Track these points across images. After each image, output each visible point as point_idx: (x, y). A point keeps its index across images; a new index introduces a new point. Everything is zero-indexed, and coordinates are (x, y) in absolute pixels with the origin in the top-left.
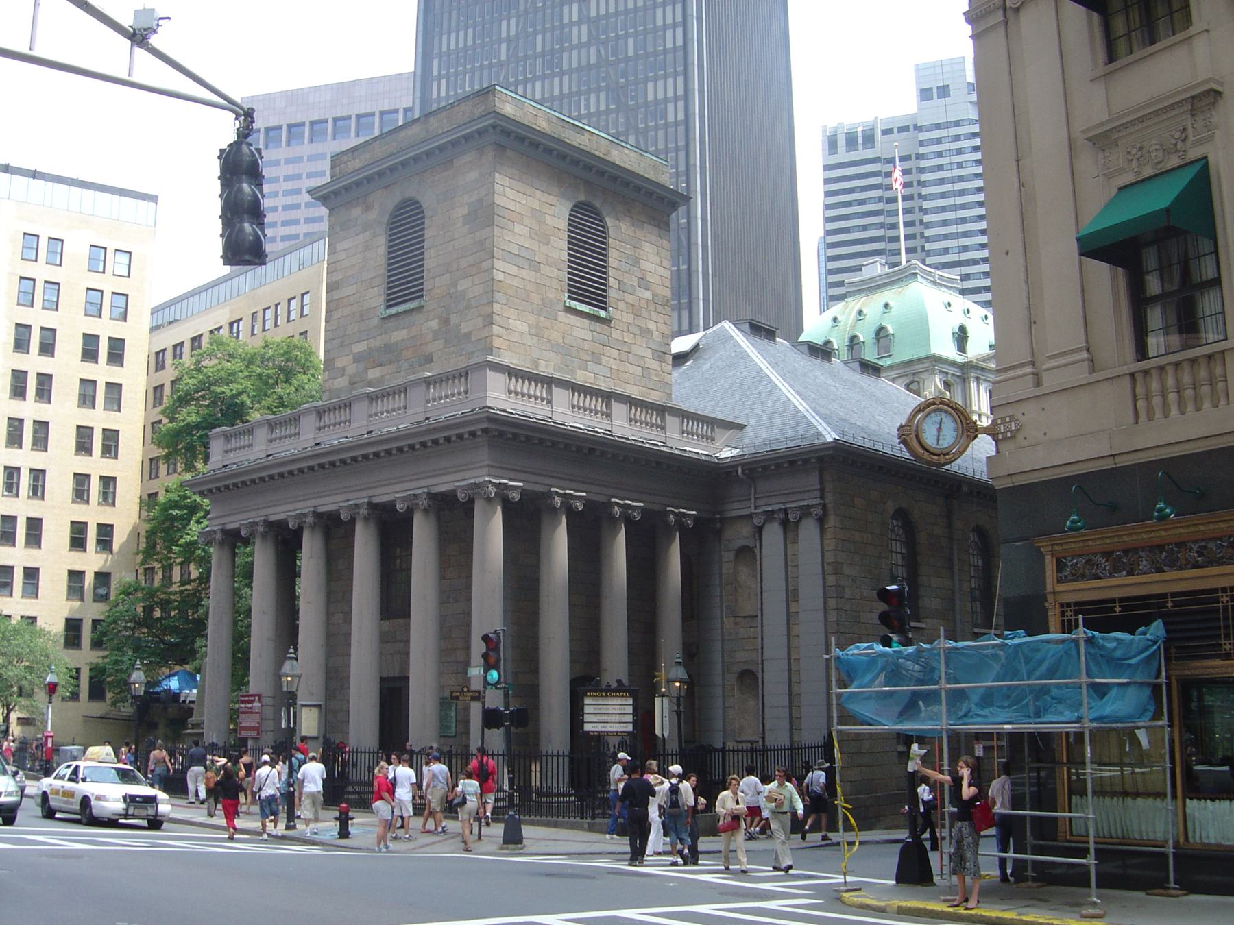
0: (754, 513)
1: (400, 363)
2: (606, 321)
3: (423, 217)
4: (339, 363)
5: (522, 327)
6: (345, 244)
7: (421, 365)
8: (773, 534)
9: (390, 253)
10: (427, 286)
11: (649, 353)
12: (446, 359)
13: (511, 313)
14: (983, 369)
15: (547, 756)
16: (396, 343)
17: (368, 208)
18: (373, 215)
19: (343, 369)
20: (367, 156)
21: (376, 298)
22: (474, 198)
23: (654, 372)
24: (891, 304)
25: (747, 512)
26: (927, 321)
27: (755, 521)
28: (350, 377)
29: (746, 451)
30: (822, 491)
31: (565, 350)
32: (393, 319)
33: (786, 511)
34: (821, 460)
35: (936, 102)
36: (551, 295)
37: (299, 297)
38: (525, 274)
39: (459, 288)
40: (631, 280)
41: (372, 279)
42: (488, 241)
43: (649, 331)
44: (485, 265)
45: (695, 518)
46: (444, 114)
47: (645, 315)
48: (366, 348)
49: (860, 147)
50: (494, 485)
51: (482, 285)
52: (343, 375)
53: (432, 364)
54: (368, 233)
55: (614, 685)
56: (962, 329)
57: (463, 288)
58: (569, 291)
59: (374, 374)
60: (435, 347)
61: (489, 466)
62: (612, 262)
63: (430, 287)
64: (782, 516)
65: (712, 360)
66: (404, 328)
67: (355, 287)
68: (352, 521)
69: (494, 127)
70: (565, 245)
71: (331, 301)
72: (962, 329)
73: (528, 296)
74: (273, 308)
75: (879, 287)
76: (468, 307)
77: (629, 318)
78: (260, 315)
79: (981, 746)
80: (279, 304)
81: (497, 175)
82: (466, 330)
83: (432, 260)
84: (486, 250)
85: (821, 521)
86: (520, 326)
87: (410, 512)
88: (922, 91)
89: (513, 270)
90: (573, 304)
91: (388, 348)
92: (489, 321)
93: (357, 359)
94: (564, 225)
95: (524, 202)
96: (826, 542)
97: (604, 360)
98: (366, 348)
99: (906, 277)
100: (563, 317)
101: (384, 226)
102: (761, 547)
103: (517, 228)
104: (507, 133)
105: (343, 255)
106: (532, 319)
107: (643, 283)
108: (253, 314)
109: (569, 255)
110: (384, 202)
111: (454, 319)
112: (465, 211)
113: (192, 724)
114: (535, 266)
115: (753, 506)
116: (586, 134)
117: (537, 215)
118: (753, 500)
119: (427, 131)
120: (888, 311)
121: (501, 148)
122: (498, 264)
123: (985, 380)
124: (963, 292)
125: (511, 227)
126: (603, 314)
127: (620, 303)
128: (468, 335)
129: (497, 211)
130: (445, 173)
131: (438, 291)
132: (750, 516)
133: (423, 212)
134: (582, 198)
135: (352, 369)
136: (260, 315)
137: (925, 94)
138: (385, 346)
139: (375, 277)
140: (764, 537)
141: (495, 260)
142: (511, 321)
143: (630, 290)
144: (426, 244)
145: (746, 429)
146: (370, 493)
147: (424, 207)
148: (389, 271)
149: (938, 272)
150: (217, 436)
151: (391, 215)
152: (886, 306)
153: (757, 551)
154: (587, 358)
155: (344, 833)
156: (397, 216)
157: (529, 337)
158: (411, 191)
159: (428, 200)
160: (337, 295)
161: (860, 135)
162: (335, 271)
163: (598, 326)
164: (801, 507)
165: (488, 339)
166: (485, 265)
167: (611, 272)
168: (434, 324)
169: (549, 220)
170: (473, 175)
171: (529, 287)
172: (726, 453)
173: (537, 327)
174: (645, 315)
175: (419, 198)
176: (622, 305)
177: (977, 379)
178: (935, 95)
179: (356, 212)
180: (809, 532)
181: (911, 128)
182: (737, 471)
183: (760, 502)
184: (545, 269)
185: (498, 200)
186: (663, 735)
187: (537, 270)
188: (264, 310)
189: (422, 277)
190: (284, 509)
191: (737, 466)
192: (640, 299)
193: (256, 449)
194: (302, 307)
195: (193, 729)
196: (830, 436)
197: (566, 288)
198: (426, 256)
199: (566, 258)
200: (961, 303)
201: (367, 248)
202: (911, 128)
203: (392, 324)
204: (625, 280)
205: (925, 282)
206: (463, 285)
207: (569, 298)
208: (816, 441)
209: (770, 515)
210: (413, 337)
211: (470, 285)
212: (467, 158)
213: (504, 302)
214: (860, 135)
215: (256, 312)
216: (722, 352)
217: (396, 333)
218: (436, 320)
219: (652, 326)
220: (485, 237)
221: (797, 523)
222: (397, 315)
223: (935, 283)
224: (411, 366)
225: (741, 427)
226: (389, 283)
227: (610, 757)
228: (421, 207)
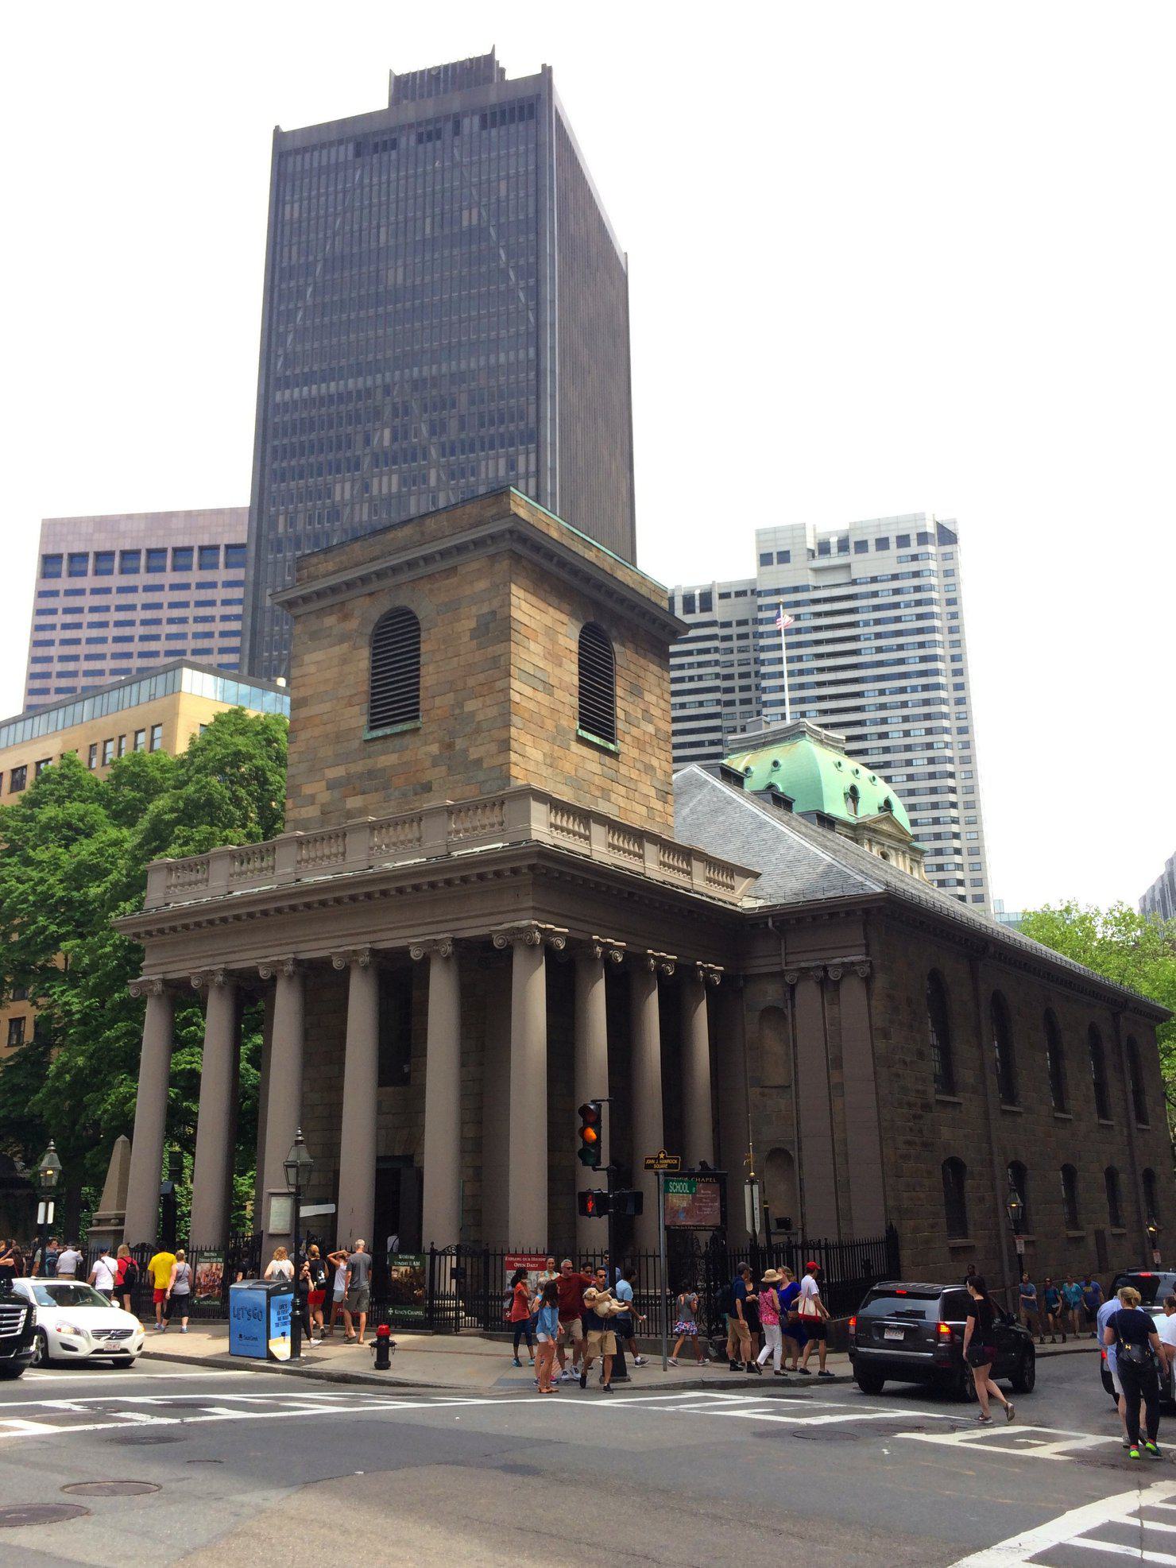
0: (787, 970)
2: (614, 755)
3: (419, 629)
4: (307, 790)
5: (535, 754)
6: (319, 656)
7: (416, 794)
8: (808, 995)
9: (374, 668)
10: (423, 706)
11: (652, 792)
12: (449, 788)
13: (526, 739)
14: (875, 831)
15: (647, 1256)
16: (384, 769)
17: (346, 617)
18: (353, 624)
19: (313, 797)
20: (344, 558)
21: (357, 717)
22: (485, 609)
23: (657, 813)
24: (781, 762)
25: (777, 969)
26: (820, 781)
27: (788, 979)
29: (775, 902)
30: (867, 946)
31: (576, 783)
33: (825, 969)
34: (867, 912)
35: (775, 566)
36: (564, 723)
37: (149, 730)
38: (540, 696)
39: (466, 709)
40: (636, 712)
42: (502, 658)
43: (653, 768)
44: (500, 685)
45: (721, 974)
46: (444, 516)
47: (649, 750)
48: (344, 774)
49: (698, 610)
50: (541, 930)
51: (496, 707)
55: (698, 1168)
56: (854, 789)
58: (580, 720)
59: (354, 802)
60: (434, 775)
61: (533, 908)
62: (619, 691)
63: (428, 708)
64: (821, 974)
65: (691, 805)
67: (328, 704)
68: (347, 971)
69: (511, 532)
70: (575, 668)
71: (297, 720)
72: (854, 789)
73: (543, 722)
74: (116, 740)
75: (764, 744)
76: (478, 731)
77: (635, 753)
78: (100, 748)
79: (1022, 1241)
80: (124, 736)
81: (513, 587)
82: (475, 756)
83: (429, 676)
84: (501, 668)
85: (868, 980)
86: (535, 754)
87: (426, 962)
88: (761, 555)
89: (528, 691)
90: (582, 733)
91: (371, 774)
92: (505, 746)
93: (331, 786)
94: (574, 646)
95: (538, 618)
96: (873, 1002)
97: (613, 797)
98: (344, 774)
99: (793, 735)
100: (576, 748)
101: (368, 637)
102: (793, 1006)
103: (533, 646)
104: (523, 540)
105: (312, 669)
106: (547, 747)
107: (647, 716)
108: (91, 746)
109: (580, 680)
110: (367, 612)
111: (460, 744)
112: (473, 624)
113: (99, 1220)
114: (549, 688)
115: (784, 963)
116: (594, 550)
117: (550, 633)
118: (783, 957)
119: (422, 533)
121: (516, 558)
122: (516, 684)
123: (879, 843)
124: (850, 753)
125: (527, 644)
126: (611, 747)
127: (626, 736)
128: (478, 762)
129: (514, 625)
130: (447, 582)
131: (439, 712)
132: (781, 974)
133: (418, 623)
134: (592, 619)
135: (324, 797)
136: (100, 748)
137: (765, 559)
139: (356, 695)
140: (797, 996)
141: (512, 680)
142: (527, 748)
143: (636, 723)
144: (423, 659)
145: (761, 879)
146: (372, 937)
147: (420, 617)
148: (373, 688)
149: (825, 732)
150: (157, 868)
151: (376, 625)
152: (776, 764)
153: (788, 1012)
154: (597, 793)
155: (382, 1363)
156: (383, 627)
157: (544, 767)
158: (403, 600)
159: (424, 608)
160: (304, 712)
161: (697, 598)
162: (304, 685)
163: (607, 760)
164: (843, 964)
165: (504, 767)
166: (500, 685)
167: (619, 702)
168: (434, 749)
169: (562, 640)
170: (482, 585)
171: (544, 712)
172: (748, 904)
173: (552, 756)
174: (649, 750)
175: (412, 607)
176: (628, 739)
177: (870, 841)
178: (775, 561)
179: (330, 621)
180: (853, 993)
181: (749, 593)
182: (767, 924)
183: (791, 958)
184: (558, 693)
185: (515, 613)
186: (754, 1231)
187: (551, 695)
188: (105, 742)
189: (418, 696)
190: (250, 956)
191: (768, 916)
192: (645, 732)
193: (213, 884)
194: (152, 740)
195: (98, 1225)
196: (878, 889)
197: (577, 715)
198: (423, 672)
199: (576, 682)
200: (851, 764)
201: (344, 661)
202: (749, 593)
203: (378, 746)
204: (631, 711)
205: (812, 740)
206: (470, 706)
207: (581, 727)
208: (861, 892)
209: (804, 972)
211: (481, 706)
212: (475, 565)
213: (521, 727)
214: (697, 598)
215: (95, 745)
216: (699, 797)
217: (383, 757)
218: (437, 745)
219: (655, 763)
220: (499, 653)
221: (837, 984)
222: (385, 737)
223: (821, 741)
224: (404, 795)
225: (757, 875)
226: (373, 701)
227: (702, 1258)
228: (415, 617)
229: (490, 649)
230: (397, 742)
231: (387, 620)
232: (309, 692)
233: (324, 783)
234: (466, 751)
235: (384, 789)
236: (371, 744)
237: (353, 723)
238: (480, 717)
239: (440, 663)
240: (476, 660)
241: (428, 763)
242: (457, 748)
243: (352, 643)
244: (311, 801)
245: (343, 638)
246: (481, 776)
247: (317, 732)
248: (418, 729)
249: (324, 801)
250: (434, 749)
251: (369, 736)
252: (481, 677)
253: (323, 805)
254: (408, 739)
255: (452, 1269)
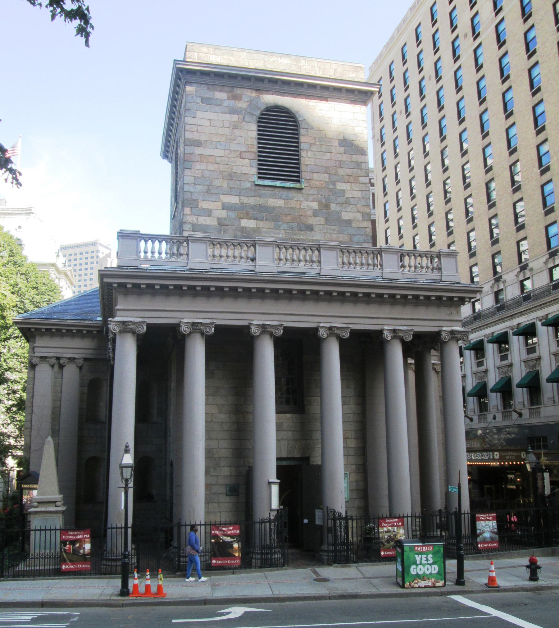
1: (279, 223)
4: (204, 205)
6: (212, 116)
7: (301, 230)
16: (274, 208)
17: (235, 98)
18: (242, 105)
28: (219, 219)
32: (270, 189)
41: (241, 152)
48: (238, 202)
52: (210, 215)
53: (313, 233)
54: (236, 116)
57: (342, 188)
66: (281, 198)
91: (262, 208)
111: (333, 207)
120: (20, 230)
128: (349, 222)
131: (317, 183)
135: (223, 214)
138: (260, 206)
139: (245, 152)
152: (20, 227)
168: (315, 205)
179: (221, 95)
198: (303, 154)
203: (268, 191)
210: (292, 208)
217: (272, 200)
229: (354, 157)
230: (284, 193)
231: (267, 111)
232: (203, 138)
233: (220, 204)
234: (339, 212)
235: (273, 220)
236: (261, 188)
237: (246, 170)
238: (348, 194)
239: (317, 153)
240: (343, 159)
241: (310, 213)
242: (332, 209)
243: (241, 117)
244: (209, 213)
245: (233, 111)
246: (351, 231)
247: (212, 167)
248: (301, 189)
249: (220, 216)
250: (315, 205)
251: (261, 182)
252: (349, 171)
253: (219, 219)
254: (292, 194)
255: (437, 524)
